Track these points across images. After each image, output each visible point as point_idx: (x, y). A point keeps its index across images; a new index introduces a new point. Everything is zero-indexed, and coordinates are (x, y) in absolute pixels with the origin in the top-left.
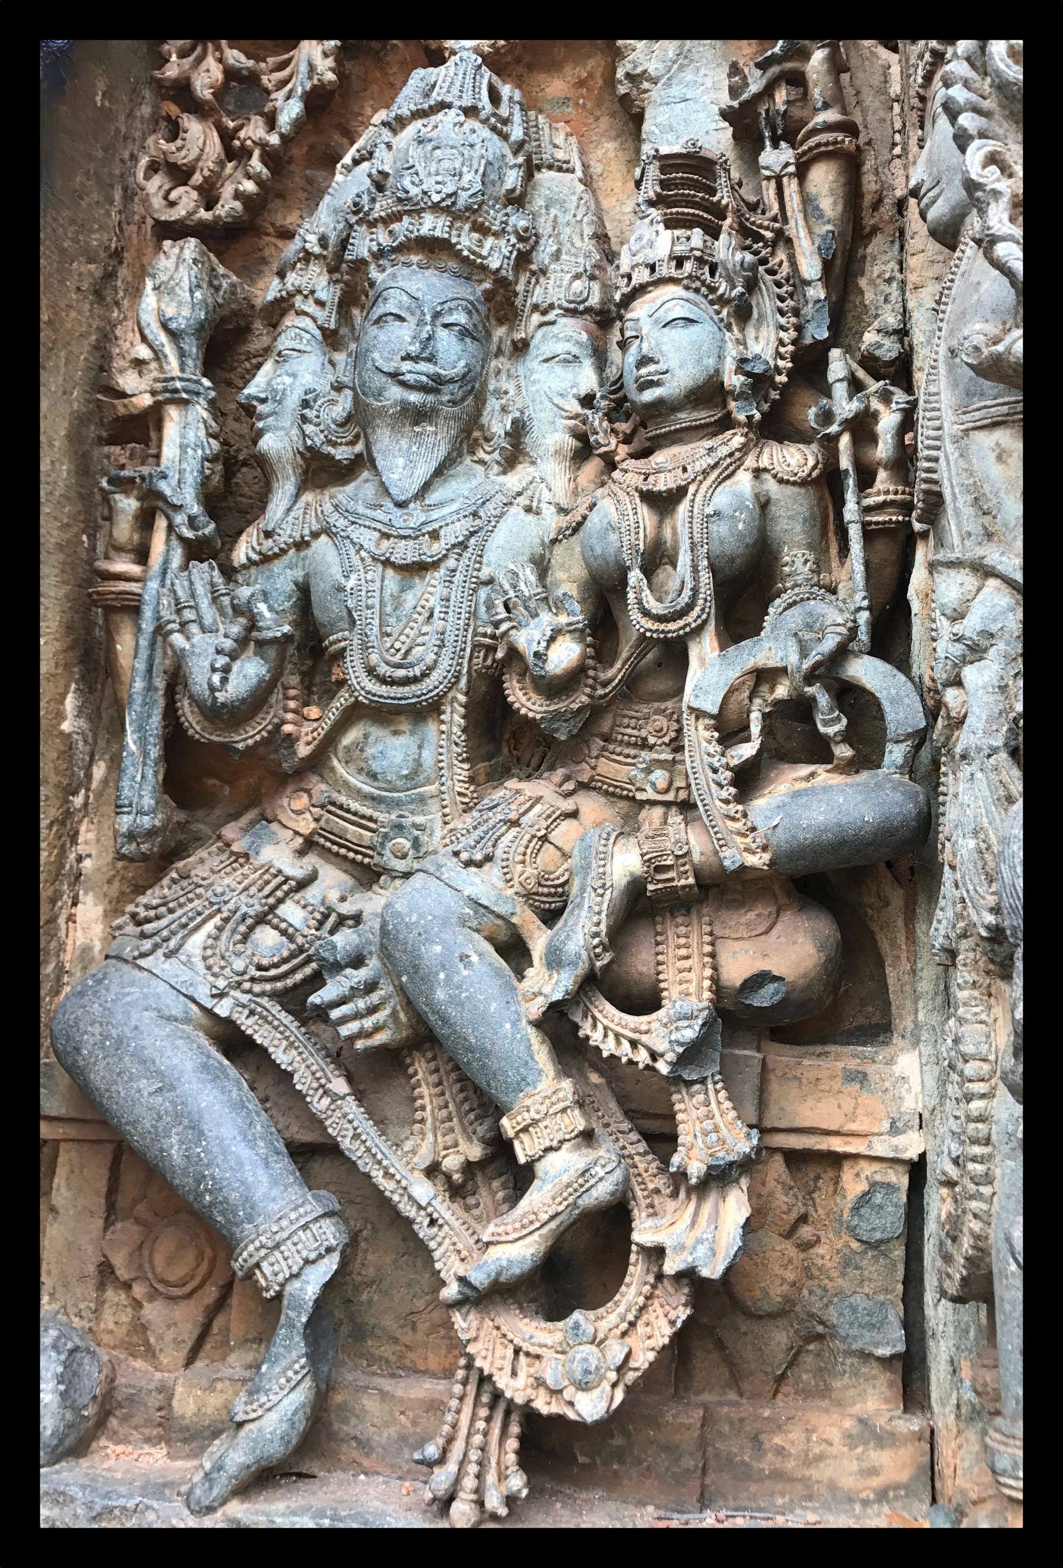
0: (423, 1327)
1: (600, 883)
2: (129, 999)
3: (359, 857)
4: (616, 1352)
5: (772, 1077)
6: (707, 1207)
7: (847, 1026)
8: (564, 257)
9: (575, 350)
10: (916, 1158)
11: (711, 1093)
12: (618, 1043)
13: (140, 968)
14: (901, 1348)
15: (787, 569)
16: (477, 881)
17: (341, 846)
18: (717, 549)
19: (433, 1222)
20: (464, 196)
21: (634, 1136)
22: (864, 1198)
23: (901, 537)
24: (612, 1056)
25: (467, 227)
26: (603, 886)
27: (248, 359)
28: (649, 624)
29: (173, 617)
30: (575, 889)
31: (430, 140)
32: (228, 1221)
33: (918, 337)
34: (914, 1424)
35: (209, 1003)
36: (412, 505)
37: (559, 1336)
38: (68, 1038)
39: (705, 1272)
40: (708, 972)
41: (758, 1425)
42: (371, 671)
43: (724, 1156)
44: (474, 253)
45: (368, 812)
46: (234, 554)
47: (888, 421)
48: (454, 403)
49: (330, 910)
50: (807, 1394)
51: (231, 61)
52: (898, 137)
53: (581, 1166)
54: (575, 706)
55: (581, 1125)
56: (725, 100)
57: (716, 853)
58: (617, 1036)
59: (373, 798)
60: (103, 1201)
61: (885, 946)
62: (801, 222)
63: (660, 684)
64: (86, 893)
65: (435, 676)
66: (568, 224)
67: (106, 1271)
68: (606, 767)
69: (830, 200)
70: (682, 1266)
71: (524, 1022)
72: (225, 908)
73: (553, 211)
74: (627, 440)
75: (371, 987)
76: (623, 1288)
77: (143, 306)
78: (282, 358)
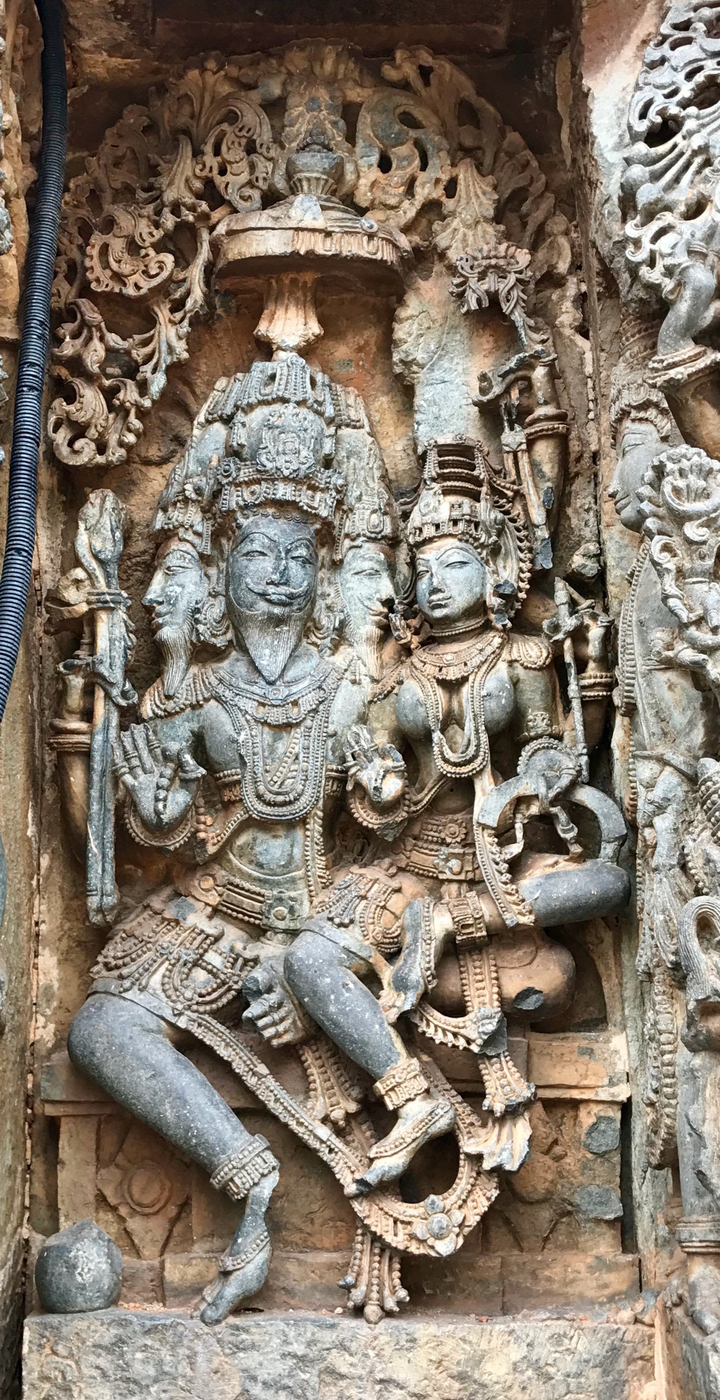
0: (318, 1221)
1: (428, 936)
2: (122, 1019)
3: (252, 920)
4: (458, 1216)
5: (533, 1054)
6: (506, 1130)
7: (577, 1020)
8: (364, 497)
9: (377, 567)
10: (625, 1100)
11: (504, 1063)
12: (445, 1035)
13: (125, 999)
14: (620, 1213)
15: (531, 724)
16: (347, 936)
17: (238, 912)
18: (490, 717)
19: (331, 1151)
20: (303, 467)
21: (454, 1093)
22: (594, 1127)
23: (605, 703)
24: (442, 1043)
25: (305, 488)
26: (430, 939)
27: (129, 559)
28: (450, 769)
29: (125, 763)
30: (408, 938)
31: (277, 427)
32: (209, 1154)
33: (611, 562)
34: (630, 1257)
35: (173, 1020)
36: (278, 683)
37: (422, 1210)
38: (85, 1047)
39: (508, 1167)
40: (496, 989)
41: (535, 1266)
42: (259, 797)
43: (515, 1099)
44: (310, 507)
45: (258, 889)
46: (143, 709)
47: (595, 632)
48: (300, 610)
49: (238, 956)
50: (563, 1248)
51: (112, 344)
52: (591, 405)
53: (429, 1109)
54: (399, 819)
55: (425, 1085)
56: (476, 395)
57: (500, 915)
58: (444, 1030)
59: (260, 880)
60: (93, 1154)
61: (601, 969)
62: (531, 483)
63: (453, 803)
64: (44, 948)
65: (303, 799)
66: (362, 468)
67: (101, 1200)
68: (417, 857)
69: (549, 466)
70: (495, 1164)
71: (386, 1024)
72: (171, 957)
73: (353, 460)
74: (417, 632)
75: (280, 1005)
76: (457, 1181)
77: (79, 542)
78: (170, 573)
